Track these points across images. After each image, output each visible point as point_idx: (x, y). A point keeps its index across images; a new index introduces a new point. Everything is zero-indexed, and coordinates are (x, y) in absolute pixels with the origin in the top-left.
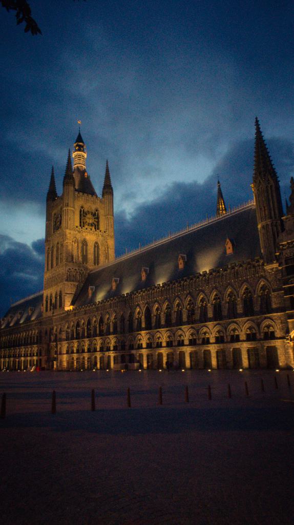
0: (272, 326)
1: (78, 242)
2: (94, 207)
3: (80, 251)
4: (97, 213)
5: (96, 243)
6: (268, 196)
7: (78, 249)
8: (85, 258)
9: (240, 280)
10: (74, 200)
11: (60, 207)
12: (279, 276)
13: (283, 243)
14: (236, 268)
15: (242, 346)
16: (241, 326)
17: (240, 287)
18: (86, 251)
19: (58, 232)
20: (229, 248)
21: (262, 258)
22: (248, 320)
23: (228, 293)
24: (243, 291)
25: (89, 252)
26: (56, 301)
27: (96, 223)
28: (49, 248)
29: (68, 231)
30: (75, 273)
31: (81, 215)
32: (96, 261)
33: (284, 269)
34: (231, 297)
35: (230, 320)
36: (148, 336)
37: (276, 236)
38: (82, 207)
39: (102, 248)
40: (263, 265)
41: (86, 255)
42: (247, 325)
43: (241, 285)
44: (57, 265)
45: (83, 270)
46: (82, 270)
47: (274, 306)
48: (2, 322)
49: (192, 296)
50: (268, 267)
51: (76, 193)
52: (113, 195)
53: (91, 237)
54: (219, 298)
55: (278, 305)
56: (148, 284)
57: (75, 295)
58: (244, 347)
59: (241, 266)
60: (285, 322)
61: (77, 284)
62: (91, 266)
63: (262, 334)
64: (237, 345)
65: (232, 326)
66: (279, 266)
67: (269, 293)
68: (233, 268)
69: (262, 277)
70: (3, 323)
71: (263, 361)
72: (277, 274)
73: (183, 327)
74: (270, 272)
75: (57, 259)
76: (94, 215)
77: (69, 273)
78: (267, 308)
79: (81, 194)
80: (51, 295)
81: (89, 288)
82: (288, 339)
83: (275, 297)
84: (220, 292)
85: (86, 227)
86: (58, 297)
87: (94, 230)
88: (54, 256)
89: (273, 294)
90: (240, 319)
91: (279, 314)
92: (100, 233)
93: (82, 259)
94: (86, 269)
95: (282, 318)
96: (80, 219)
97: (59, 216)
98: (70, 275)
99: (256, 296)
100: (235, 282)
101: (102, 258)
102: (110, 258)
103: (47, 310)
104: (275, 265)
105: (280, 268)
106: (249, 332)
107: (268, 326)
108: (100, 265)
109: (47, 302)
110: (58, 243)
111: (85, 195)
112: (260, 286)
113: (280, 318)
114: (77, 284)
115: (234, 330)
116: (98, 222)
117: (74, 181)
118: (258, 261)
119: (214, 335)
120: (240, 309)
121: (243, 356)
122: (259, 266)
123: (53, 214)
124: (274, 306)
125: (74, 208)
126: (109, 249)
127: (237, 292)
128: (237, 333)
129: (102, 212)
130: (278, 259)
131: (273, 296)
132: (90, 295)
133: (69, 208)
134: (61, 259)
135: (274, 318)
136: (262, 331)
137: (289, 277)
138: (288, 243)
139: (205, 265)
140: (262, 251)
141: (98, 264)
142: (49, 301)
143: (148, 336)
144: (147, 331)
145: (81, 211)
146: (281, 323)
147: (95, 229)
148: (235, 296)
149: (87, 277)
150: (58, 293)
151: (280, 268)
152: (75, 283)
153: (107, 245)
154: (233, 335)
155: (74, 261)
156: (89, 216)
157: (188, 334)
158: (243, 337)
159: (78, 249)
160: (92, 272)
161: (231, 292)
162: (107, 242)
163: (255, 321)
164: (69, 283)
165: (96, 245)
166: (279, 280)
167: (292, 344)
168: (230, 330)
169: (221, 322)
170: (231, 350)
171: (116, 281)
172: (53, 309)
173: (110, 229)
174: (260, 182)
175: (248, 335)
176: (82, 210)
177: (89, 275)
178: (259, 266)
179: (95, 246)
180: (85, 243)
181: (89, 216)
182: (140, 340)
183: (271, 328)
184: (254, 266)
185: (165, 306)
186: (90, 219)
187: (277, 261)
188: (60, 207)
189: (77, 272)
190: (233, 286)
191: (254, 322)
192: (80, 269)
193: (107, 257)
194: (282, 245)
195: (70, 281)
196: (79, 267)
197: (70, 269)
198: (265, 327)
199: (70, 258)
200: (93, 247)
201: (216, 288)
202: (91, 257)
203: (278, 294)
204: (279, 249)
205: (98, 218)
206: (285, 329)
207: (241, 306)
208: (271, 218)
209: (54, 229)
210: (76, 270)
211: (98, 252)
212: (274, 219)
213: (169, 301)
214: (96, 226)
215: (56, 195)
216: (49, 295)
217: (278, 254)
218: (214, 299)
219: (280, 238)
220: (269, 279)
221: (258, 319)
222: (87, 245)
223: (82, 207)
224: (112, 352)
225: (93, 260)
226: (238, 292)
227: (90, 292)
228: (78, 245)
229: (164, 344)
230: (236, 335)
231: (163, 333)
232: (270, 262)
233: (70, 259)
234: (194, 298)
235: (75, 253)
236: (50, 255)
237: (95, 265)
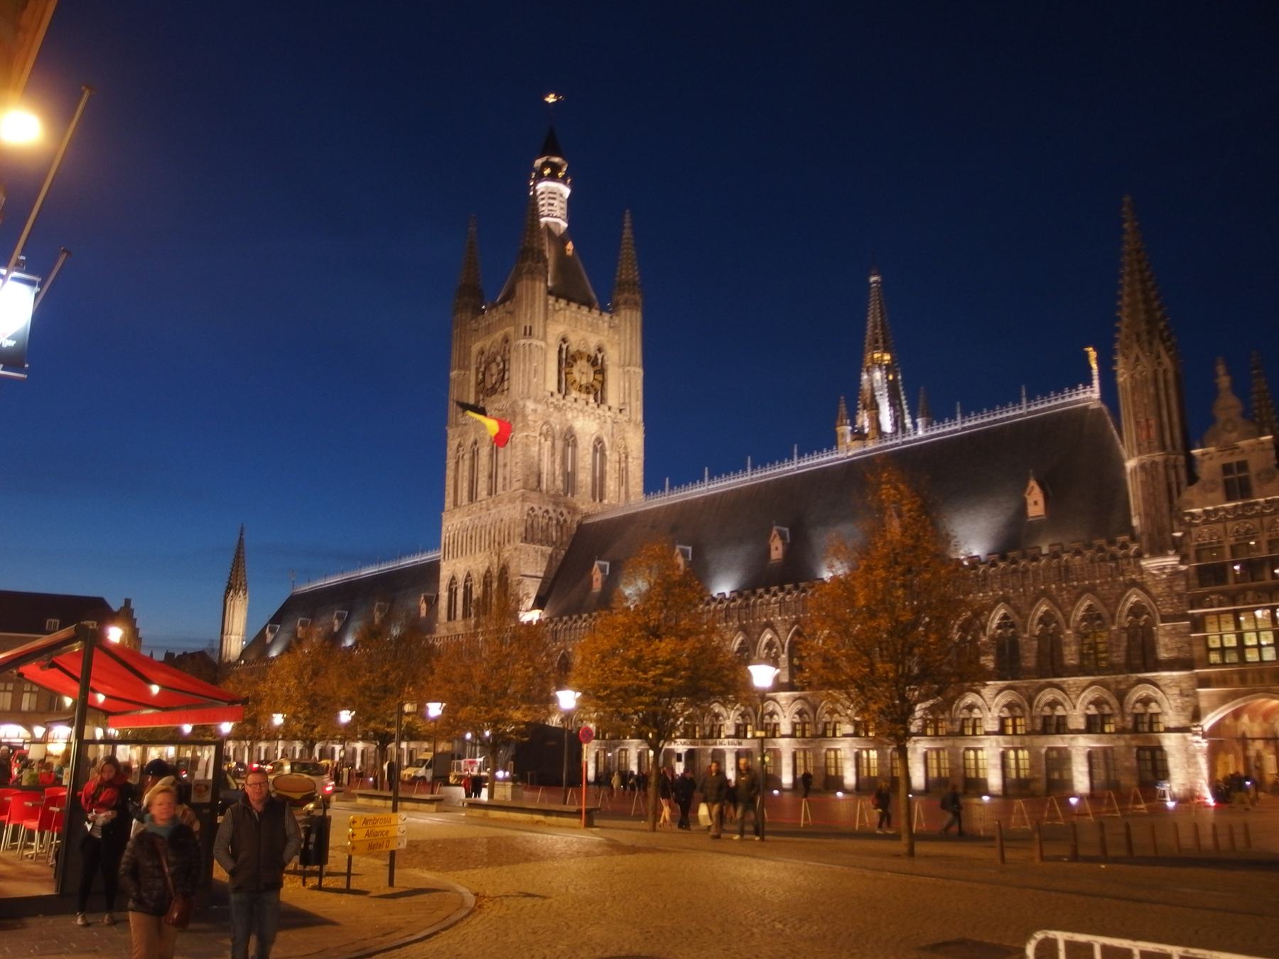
0: (1156, 702)
2: (593, 341)
4: (600, 356)
6: (1157, 396)
8: (570, 479)
9: (1075, 588)
10: (546, 318)
12: (1180, 587)
13: (1194, 510)
14: (1065, 557)
15: (1074, 743)
16: (1073, 696)
17: (1073, 604)
19: (496, 405)
20: (1036, 503)
21: (1134, 539)
22: (1092, 683)
23: (1039, 614)
24: (1080, 613)
25: (580, 464)
27: (598, 386)
28: (460, 445)
29: (530, 405)
30: (546, 521)
32: (598, 489)
33: (1192, 571)
34: (1047, 625)
35: (1043, 681)
36: (799, 706)
37: (1175, 491)
38: (564, 340)
39: (612, 456)
40: (1139, 555)
42: (1090, 695)
43: (1078, 597)
44: (490, 494)
45: (565, 512)
46: (562, 514)
47: (1163, 655)
48: (270, 637)
51: (551, 300)
53: (587, 423)
54: (1012, 625)
55: (1174, 654)
56: (795, 572)
57: (544, 579)
58: (1080, 746)
59: (1078, 552)
60: (1191, 692)
61: (549, 550)
62: (584, 503)
63: (1129, 719)
64: (1059, 741)
65: (1048, 695)
66: (1181, 562)
67: (1151, 623)
68: (1055, 555)
69: (1133, 584)
70: (273, 641)
71: (1129, 781)
72: (1174, 580)
74: (1154, 575)
75: (490, 477)
76: (593, 361)
78: (1144, 657)
79: (563, 303)
81: (596, 566)
82: (1196, 734)
83: (1168, 634)
84: (1017, 610)
85: (574, 394)
86: (495, 585)
87: (595, 405)
88: (481, 468)
89: (1162, 628)
90: (1071, 680)
91: (1175, 674)
92: (609, 413)
93: (563, 482)
94: (573, 510)
95: (1184, 685)
96: (559, 372)
97: (499, 359)
98: (532, 525)
99: (1114, 628)
100: (1060, 589)
101: (611, 484)
103: (451, 616)
104: (1171, 560)
105: (1183, 568)
106: (1093, 710)
107: (1146, 701)
108: (606, 502)
109: (452, 593)
111: (574, 306)
112: (1129, 605)
113: (1177, 683)
114: (549, 550)
115: (1053, 704)
116: (603, 383)
117: (546, 266)
118: (1124, 546)
119: (995, 713)
120: (1070, 655)
121: (1074, 768)
122: (1126, 556)
123: (475, 348)
124: (1163, 655)
126: (630, 460)
127: (1064, 615)
128: (1060, 711)
130: (1177, 546)
131: (1161, 632)
132: (597, 586)
133: (535, 342)
134: (505, 479)
135: (1160, 683)
136: (1128, 710)
137: (1206, 590)
138: (1205, 512)
140: (1135, 522)
142: (460, 592)
143: (798, 706)
144: (796, 694)
146: (1182, 694)
147: (596, 400)
148: (1057, 622)
149: (573, 532)
150: (495, 572)
151: (1183, 568)
152: (544, 548)
153: (626, 448)
154: (1050, 717)
155: (544, 487)
156: (582, 365)
159: (553, 454)
160: (590, 521)
161: (1046, 613)
162: (624, 439)
163: (1113, 686)
164: (531, 548)
166: (1179, 595)
167: (1204, 744)
168: (1042, 702)
169: (1016, 683)
170: (1043, 751)
172: (477, 615)
173: (634, 404)
174: (1137, 359)
175: (1089, 718)
176: (564, 346)
177: (580, 525)
178: (1126, 556)
180: (570, 439)
181: (582, 365)
182: (772, 714)
183: (1153, 705)
184: (1114, 558)
186: (582, 373)
187: (1177, 553)
188: (499, 336)
189: (550, 518)
190: (1052, 599)
191: (1109, 689)
192: (559, 510)
194: (1192, 515)
195: (533, 541)
196: (556, 504)
197: (532, 509)
198: (1137, 701)
199: (533, 480)
200: (591, 450)
201: (1006, 599)
202: (584, 478)
203: (1174, 628)
204: (1182, 522)
206: (1191, 709)
207: (1074, 648)
208: (1163, 447)
210: (547, 511)
212: (1170, 449)
214: (597, 391)
216: (461, 578)
217: (1178, 534)
218: (999, 627)
219: (1186, 496)
220: (1154, 591)
221: (1119, 683)
222: (575, 446)
223: (564, 340)
224: (678, 741)
225: (590, 488)
226: (1067, 617)
227: (597, 576)
230: (1058, 717)
232: (1159, 551)
235: (546, 466)
237: (594, 500)
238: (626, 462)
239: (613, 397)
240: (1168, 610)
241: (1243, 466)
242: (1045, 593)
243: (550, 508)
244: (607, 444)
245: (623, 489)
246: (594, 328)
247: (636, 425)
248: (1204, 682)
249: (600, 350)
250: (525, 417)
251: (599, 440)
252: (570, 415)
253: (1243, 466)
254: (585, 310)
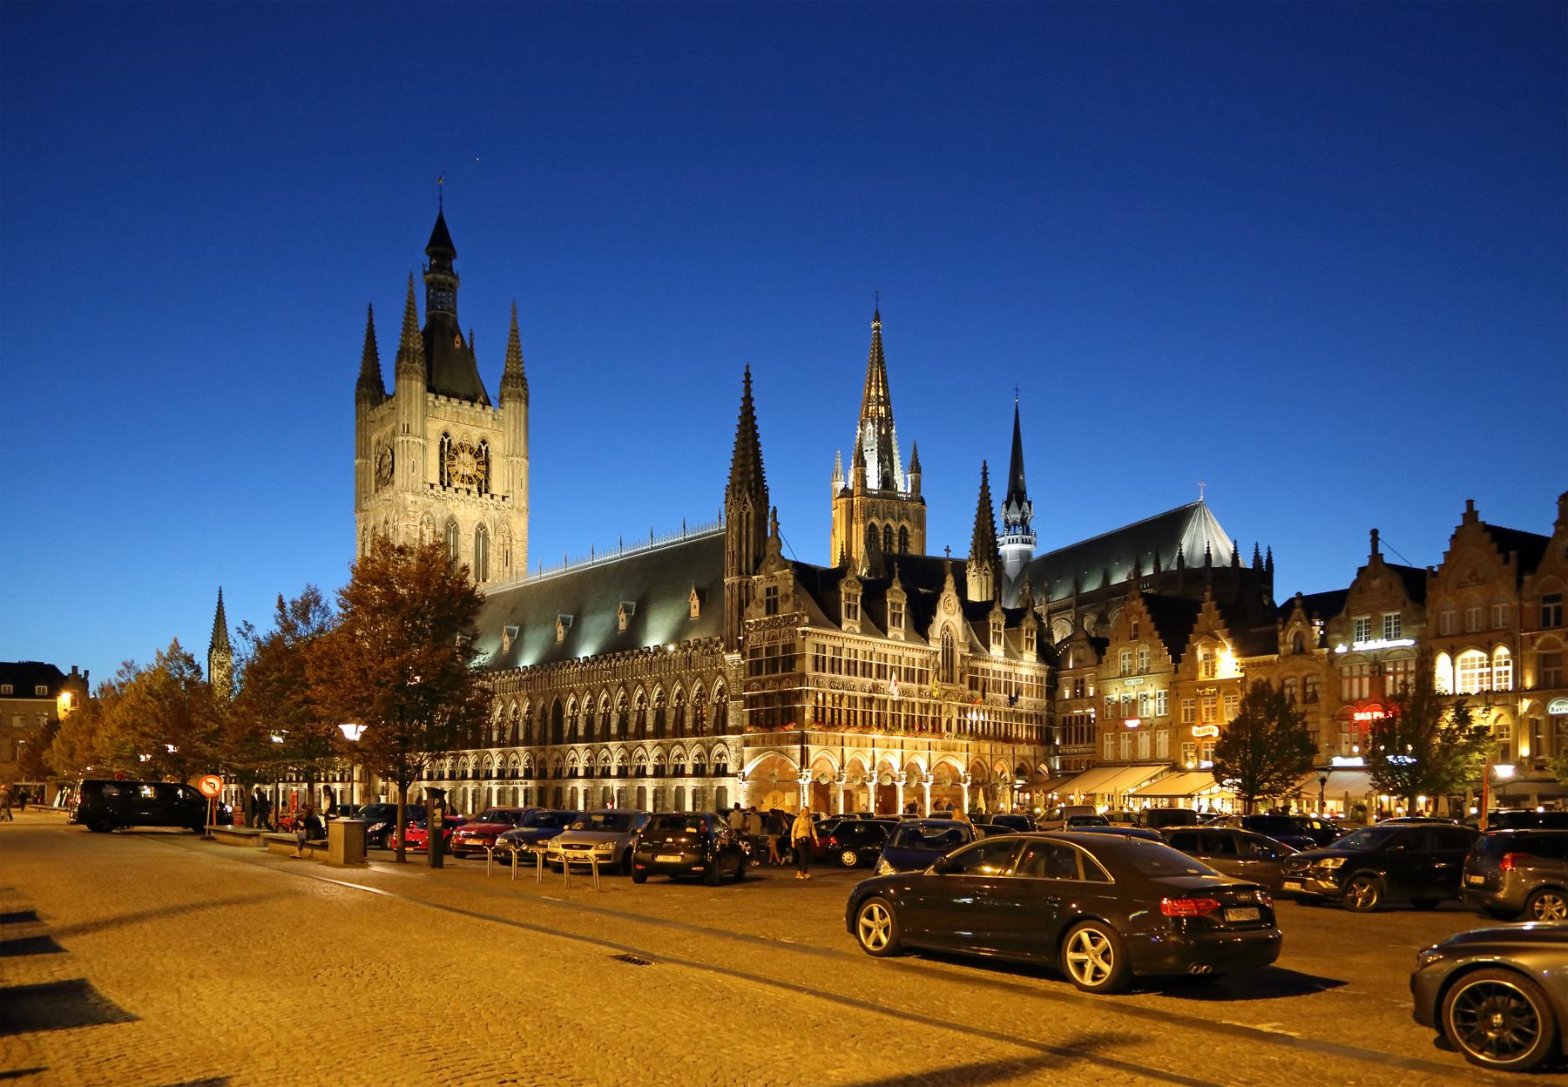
5: (482, 526)
11: (389, 429)
25: (462, 549)
27: (482, 477)
31: (442, 456)
39: (495, 541)
47: (731, 723)
49: (626, 690)
50: (728, 657)
53: (468, 511)
64: (679, 782)
65: (677, 750)
73: (610, 744)
76: (477, 454)
89: (732, 704)
96: (442, 465)
101: (494, 565)
102: (516, 563)
104: (736, 656)
110: (386, 522)
111: (455, 402)
116: (487, 473)
125: (425, 438)
139: (656, 635)
145: (442, 443)
147: (479, 490)
157: (617, 757)
158: (689, 770)
165: (481, 533)
171: (511, 633)
173: (517, 492)
179: (477, 534)
181: (466, 457)
185: (585, 703)
186: (465, 465)
187: (740, 649)
193: (507, 559)
205: (487, 463)
208: (740, 573)
209: (377, 482)
211: (485, 548)
213: (592, 693)
215: (380, 385)
222: (457, 532)
223: (446, 435)
229: (581, 773)
231: (581, 751)
234: (629, 694)
239: (497, 486)
240: (734, 692)
241: (775, 589)
242: (679, 677)
244: (490, 531)
245: (507, 569)
246: (477, 423)
247: (520, 511)
248: (747, 744)
249: (484, 442)
250: (405, 508)
251: (482, 526)
253: (775, 589)
254: (467, 404)
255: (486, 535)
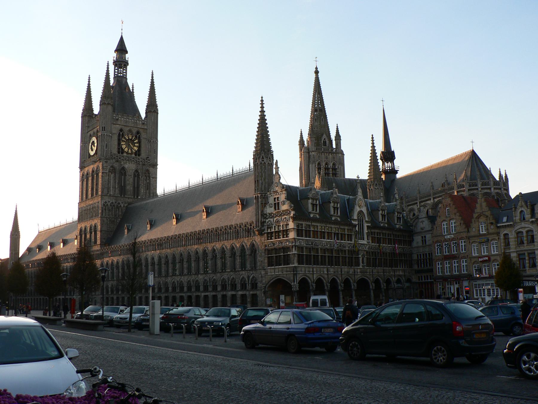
1: (115, 173)
3: (117, 181)
4: (138, 136)
5: (136, 171)
7: (115, 179)
18: (125, 182)
25: (128, 182)
26: (90, 236)
31: (119, 140)
41: (125, 186)
46: (119, 203)
52: (158, 113)
77: (104, 207)
80: (85, 229)
110: (93, 171)
129: (143, 135)
134: (96, 190)
141: (137, 197)
145: (119, 134)
153: (149, 174)
159: (115, 179)
165: (136, 174)
176: (121, 133)
222: (125, 175)
228: (115, 174)
233: (106, 191)
236: (85, 183)
238: (149, 180)
243: (114, 201)
252: (122, 163)
255: (138, 175)
